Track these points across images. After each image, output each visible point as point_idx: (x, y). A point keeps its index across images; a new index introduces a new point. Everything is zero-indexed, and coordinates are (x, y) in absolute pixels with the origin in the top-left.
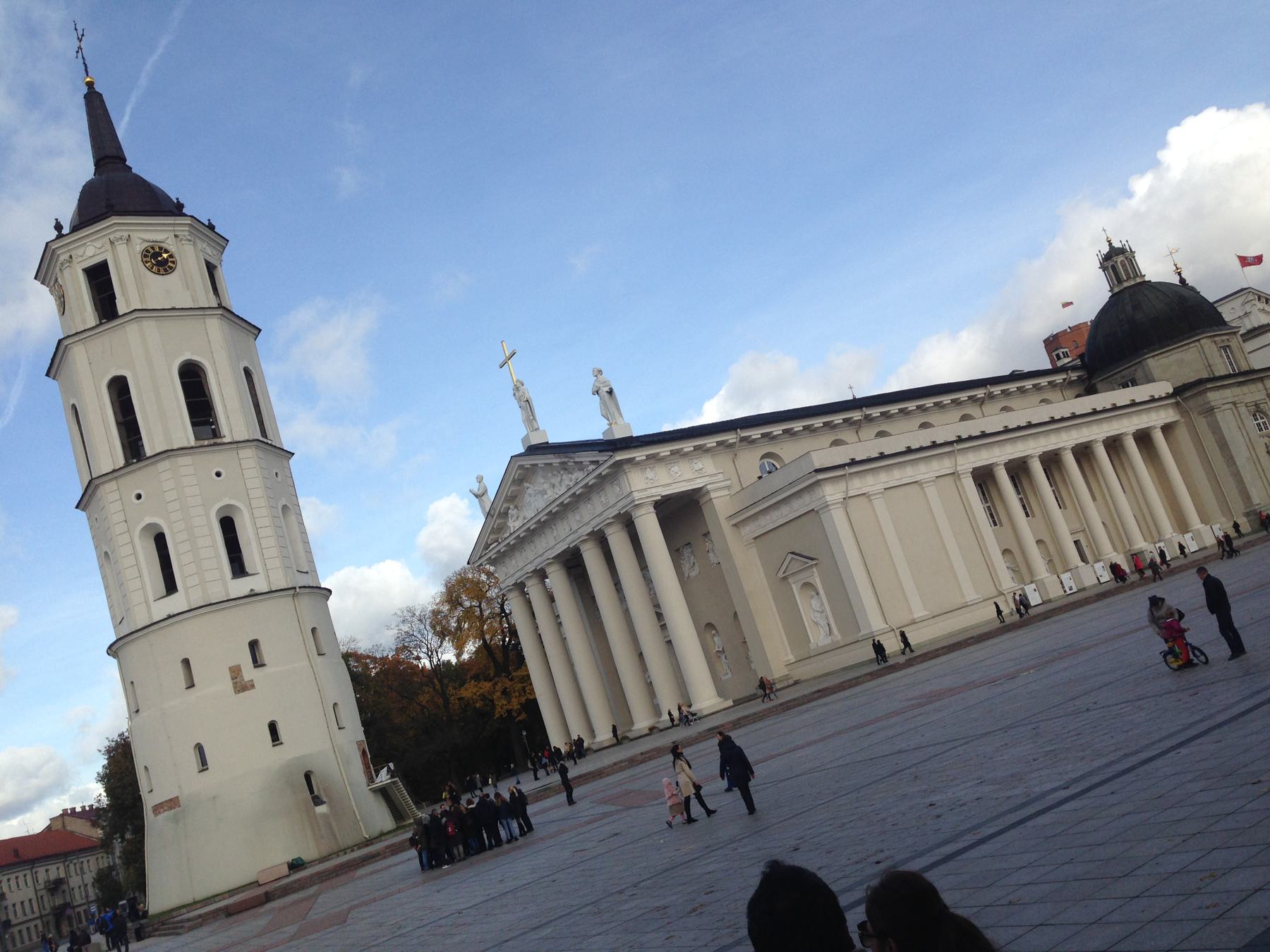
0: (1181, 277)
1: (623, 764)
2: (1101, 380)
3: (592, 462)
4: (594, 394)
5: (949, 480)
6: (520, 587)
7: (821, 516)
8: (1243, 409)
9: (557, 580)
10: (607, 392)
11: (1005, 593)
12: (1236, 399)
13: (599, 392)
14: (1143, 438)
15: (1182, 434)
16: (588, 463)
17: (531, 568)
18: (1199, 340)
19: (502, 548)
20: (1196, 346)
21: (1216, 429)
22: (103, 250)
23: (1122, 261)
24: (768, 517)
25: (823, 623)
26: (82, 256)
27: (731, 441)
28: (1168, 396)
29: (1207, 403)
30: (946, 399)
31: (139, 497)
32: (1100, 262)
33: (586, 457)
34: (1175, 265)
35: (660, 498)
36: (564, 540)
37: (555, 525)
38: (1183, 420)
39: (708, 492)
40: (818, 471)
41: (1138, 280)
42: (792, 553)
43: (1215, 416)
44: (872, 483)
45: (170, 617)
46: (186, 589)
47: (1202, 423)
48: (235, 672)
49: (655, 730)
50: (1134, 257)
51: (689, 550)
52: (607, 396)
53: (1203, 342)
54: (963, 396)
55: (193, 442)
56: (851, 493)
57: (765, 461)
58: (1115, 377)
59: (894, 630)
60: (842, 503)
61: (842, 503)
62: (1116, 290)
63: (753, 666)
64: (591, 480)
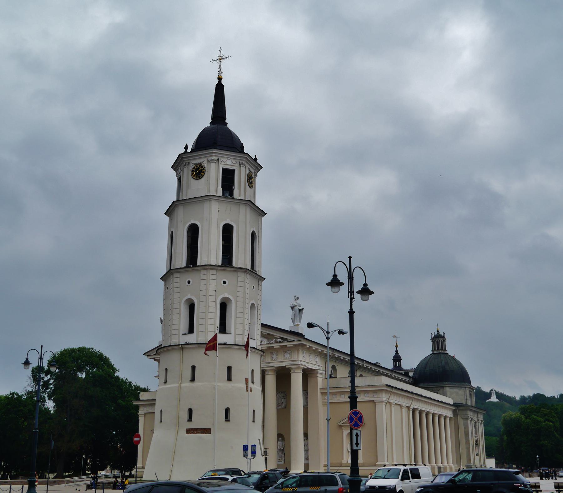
3: (281, 338)
4: (290, 307)
5: (407, 409)
7: (376, 405)
8: (473, 422)
10: (299, 309)
18: (466, 387)
20: (464, 389)
21: (466, 427)
22: (235, 165)
23: (442, 341)
24: (343, 396)
26: (224, 162)
29: (468, 415)
31: (224, 283)
34: (396, 343)
35: (306, 368)
38: (454, 418)
39: (317, 373)
40: (387, 385)
41: (445, 352)
43: (468, 421)
45: (225, 344)
46: (236, 334)
48: (247, 380)
50: (445, 341)
52: (298, 310)
53: (467, 389)
55: (250, 269)
62: (435, 352)
64: (277, 346)
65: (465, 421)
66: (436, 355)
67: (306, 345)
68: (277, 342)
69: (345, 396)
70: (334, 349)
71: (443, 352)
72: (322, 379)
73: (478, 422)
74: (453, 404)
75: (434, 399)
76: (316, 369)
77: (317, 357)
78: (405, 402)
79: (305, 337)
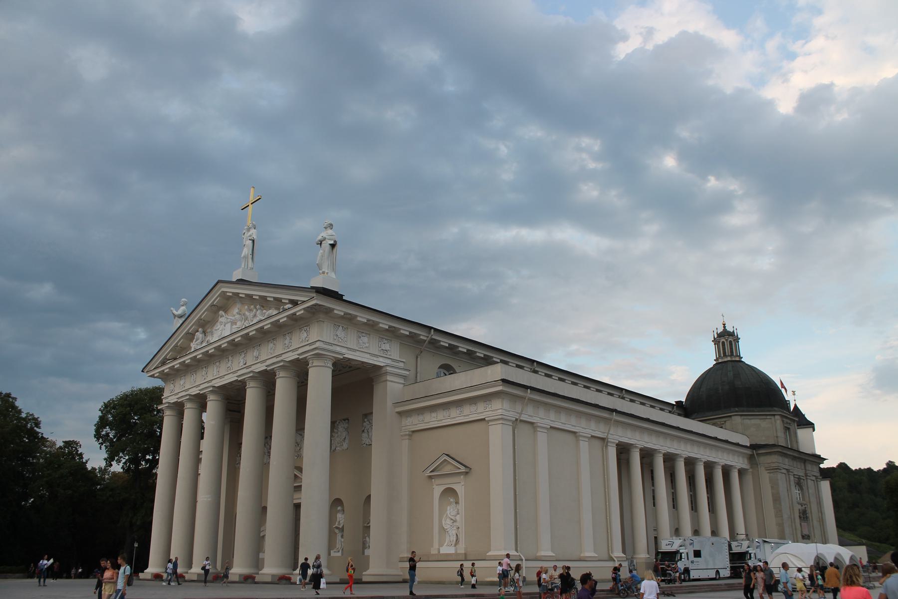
5: (597, 443)
6: (179, 408)
8: (792, 478)
10: (330, 244)
11: (615, 559)
12: (790, 468)
13: (323, 243)
14: (726, 472)
15: (749, 479)
16: (287, 301)
17: (194, 391)
18: (774, 415)
19: (176, 364)
23: (730, 341)
24: (434, 415)
25: (453, 532)
27: (422, 337)
28: (745, 447)
32: (714, 337)
33: (285, 296)
37: (232, 356)
38: (751, 470)
41: (737, 359)
42: (447, 455)
44: (543, 418)
47: (765, 476)
49: (250, 580)
50: (738, 342)
51: (346, 426)
52: (328, 248)
56: (524, 417)
57: (441, 370)
59: (522, 560)
60: (513, 422)
61: (513, 422)
62: (720, 361)
63: (367, 552)
64: (283, 318)
65: (772, 475)
66: (720, 365)
67: (333, 309)
68: (285, 310)
69: (437, 417)
70: (431, 328)
71: (734, 359)
72: (402, 385)
73: (807, 479)
74: (749, 445)
75: (649, 419)
76: (382, 365)
77: (386, 342)
78: (588, 428)
79: (344, 298)
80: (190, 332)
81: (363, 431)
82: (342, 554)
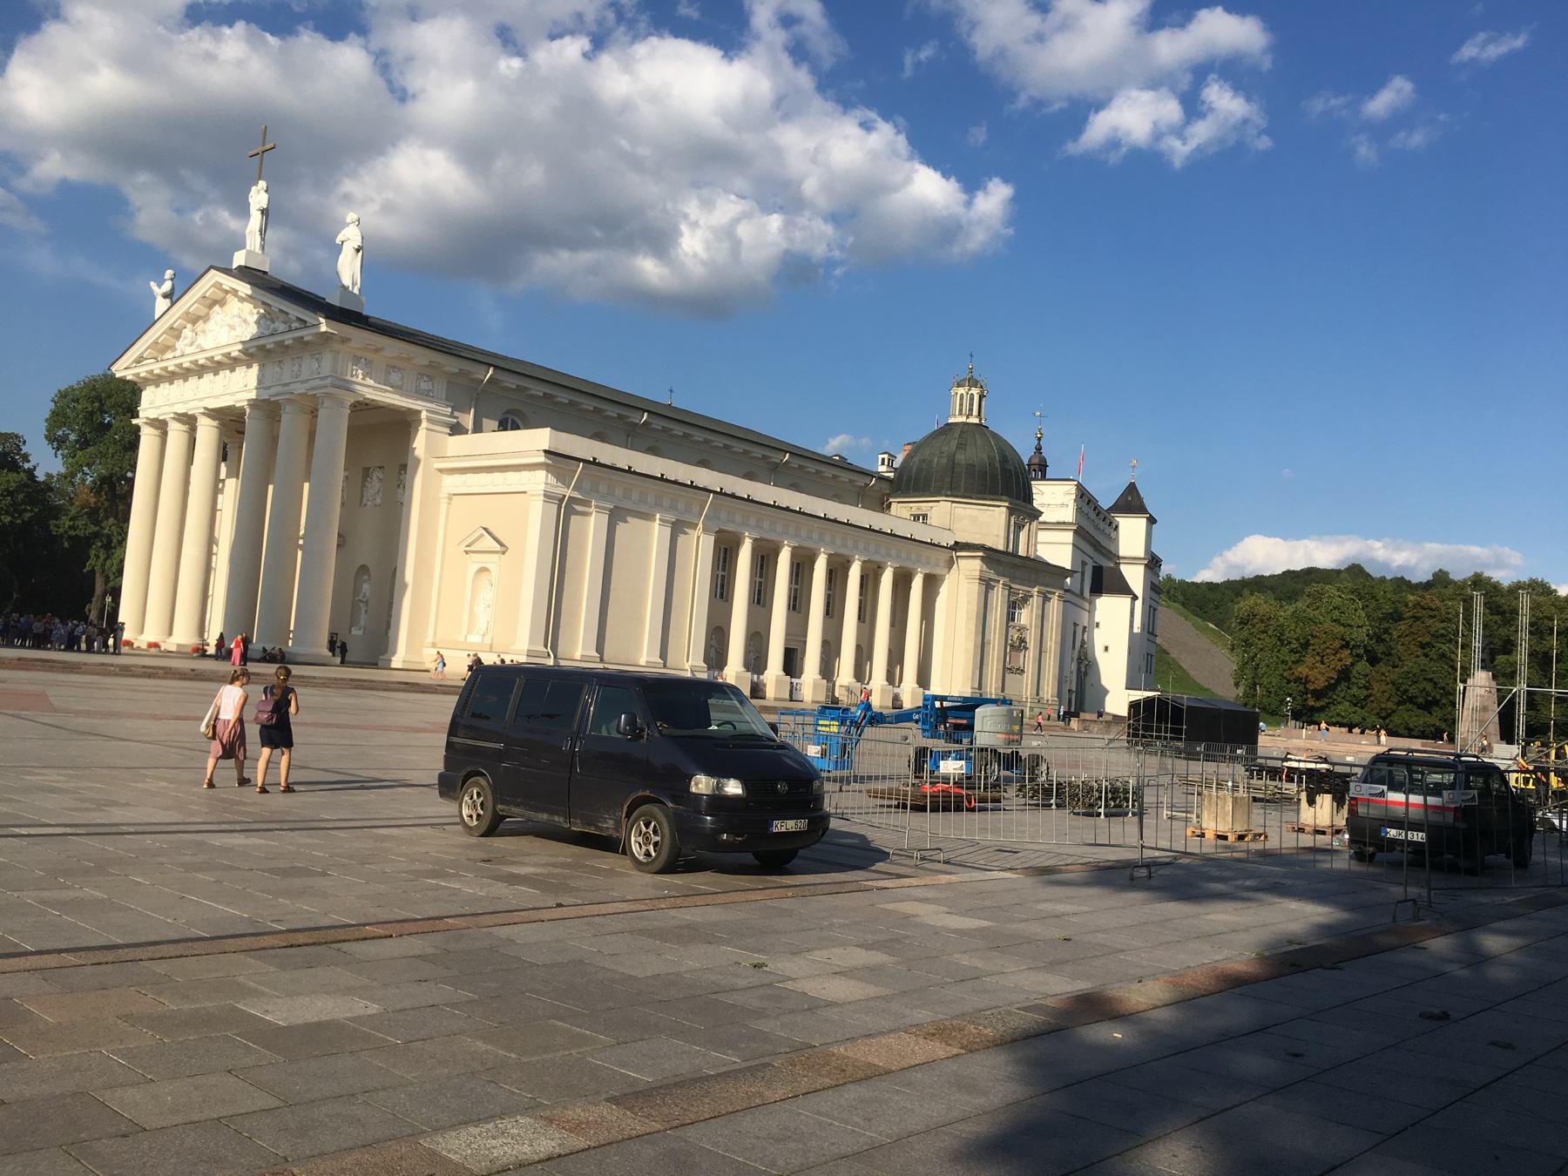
0: (1039, 444)
1: (112, 669)
2: (899, 502)
9: (207, 433)
16: (295, 319)
17: (181, 409)
19: (156, 368)
23: (972, 394)
30: (739, 447)
36: (232, 394)
42: (485, 529)
51: (381, 476)
54: (758, 452)
57: (510, 417)
58: (912, 505)
64: (288, 339)
80: (175, 326)
81: (399, 486)
82: (364, 633)
